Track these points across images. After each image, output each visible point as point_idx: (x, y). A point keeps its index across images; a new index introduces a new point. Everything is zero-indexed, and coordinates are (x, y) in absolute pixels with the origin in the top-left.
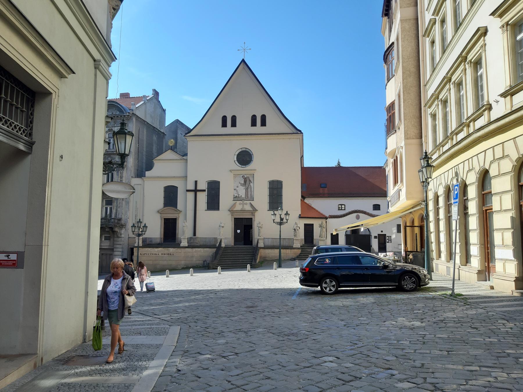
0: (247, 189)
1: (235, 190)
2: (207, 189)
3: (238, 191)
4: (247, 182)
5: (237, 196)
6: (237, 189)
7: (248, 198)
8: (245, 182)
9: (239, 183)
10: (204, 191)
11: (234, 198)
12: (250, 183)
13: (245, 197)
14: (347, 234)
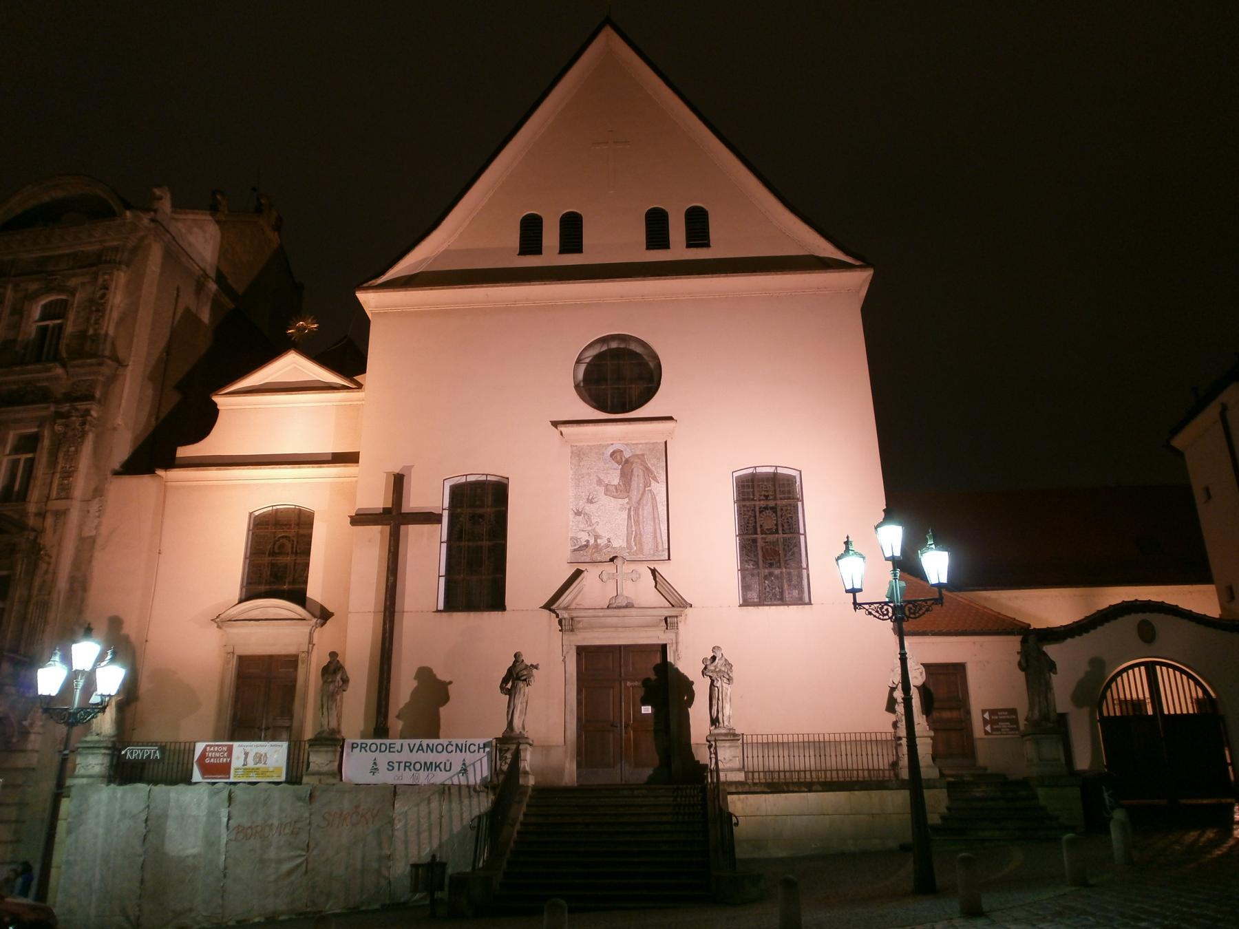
0: (637, 510)
1: (578, 513)
2: (446, 514)
3: (593, 521)
4: (635, 479)
5: (588, 541)
6: (589, 508)
7: (641, 550)
8: (626, 475)
9: (599, 482)
10: (430, 518)
11: (575, 550)
12: (647, 484)
13: (625, 545)
14: (1105, 714)
